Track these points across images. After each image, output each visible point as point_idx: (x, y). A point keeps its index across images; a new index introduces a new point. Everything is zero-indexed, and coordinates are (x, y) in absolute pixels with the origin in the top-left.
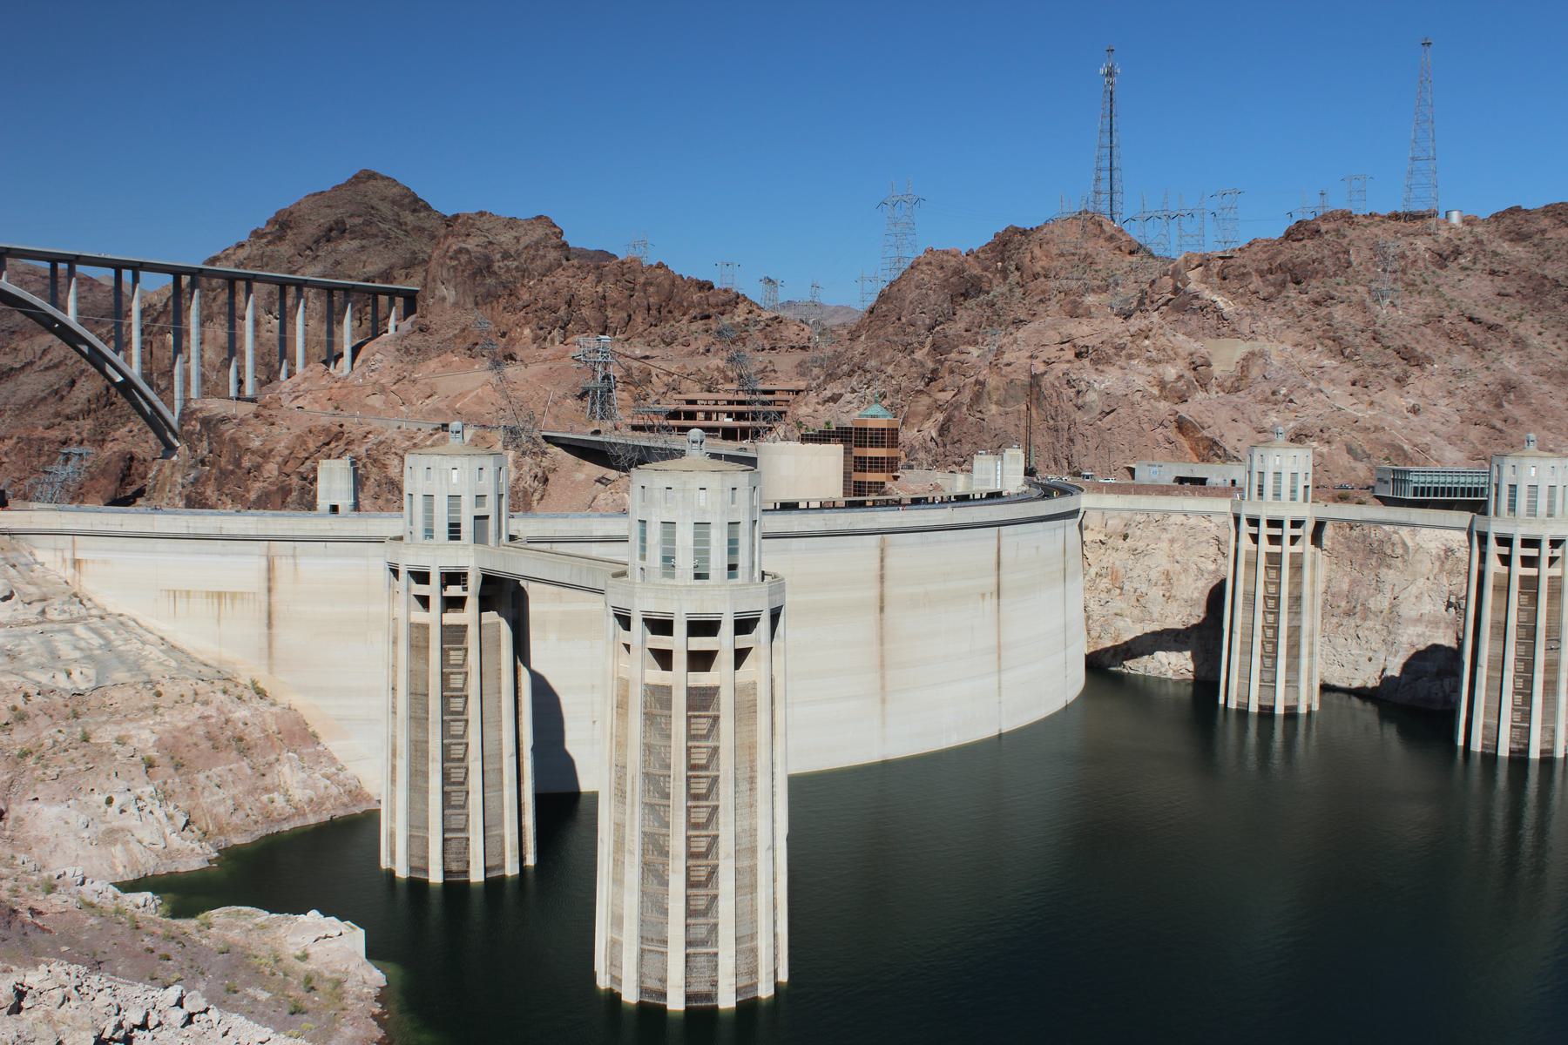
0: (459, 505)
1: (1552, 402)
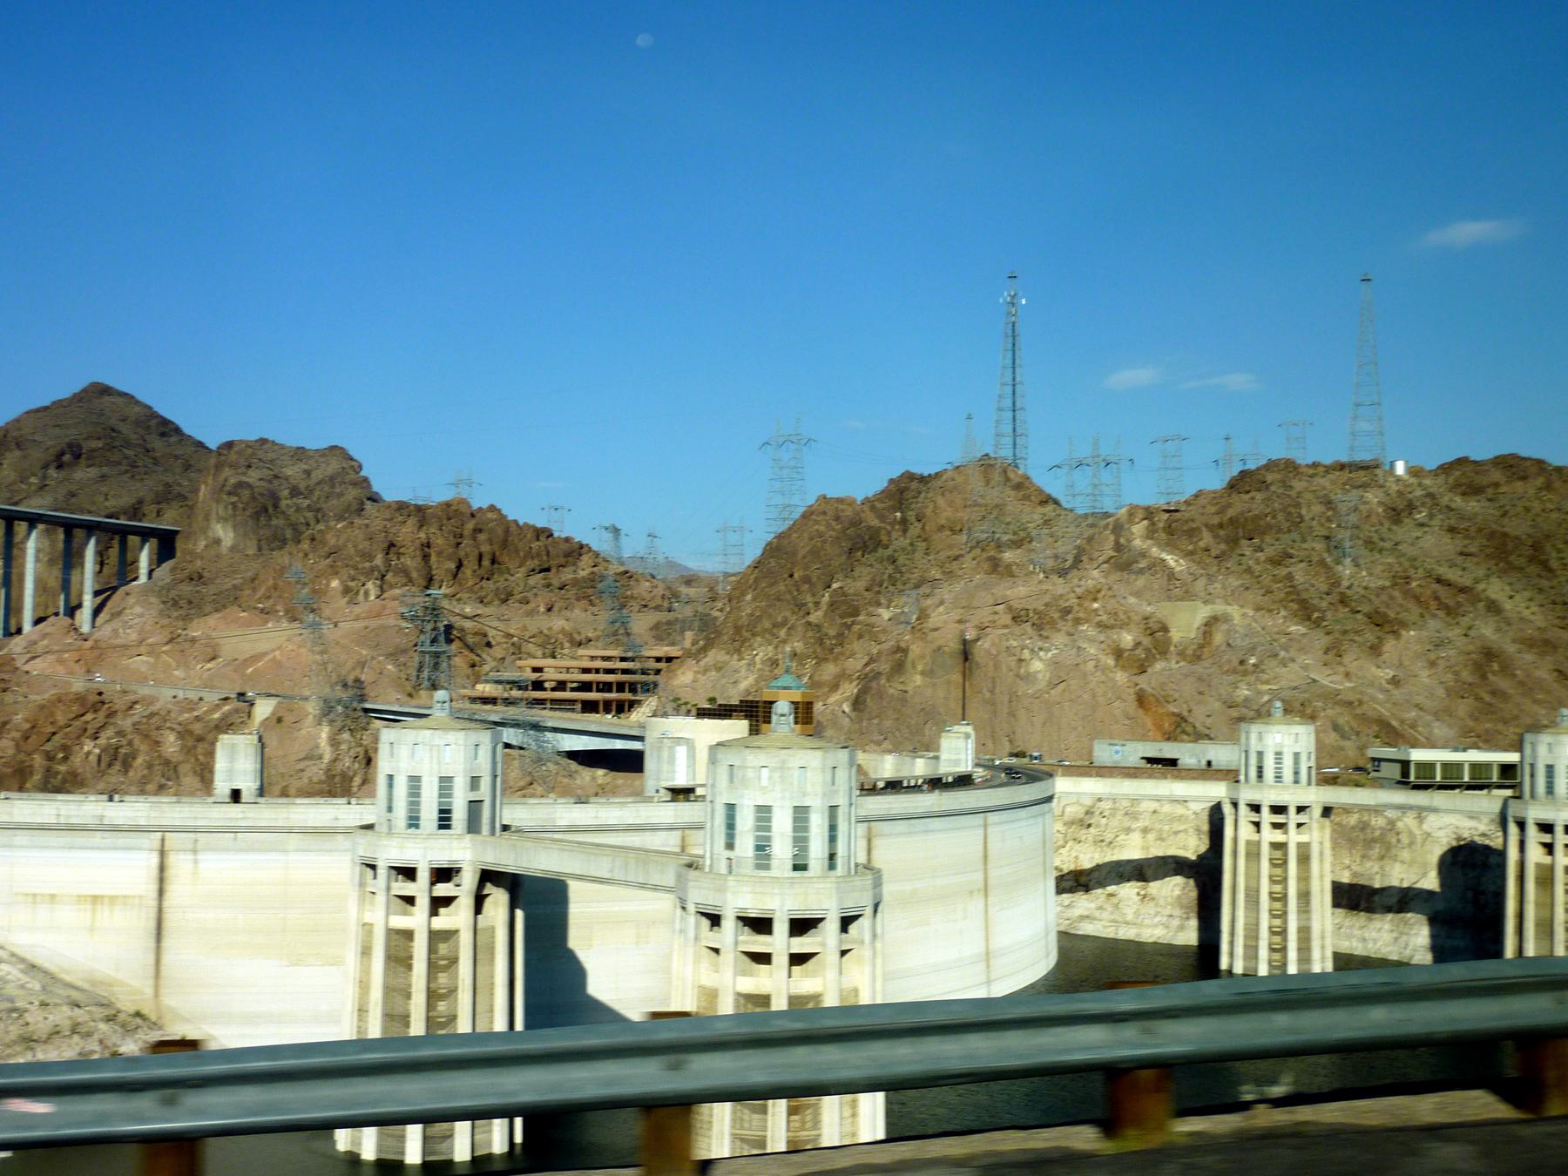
0: (451, 788)
1: (1538, 673)
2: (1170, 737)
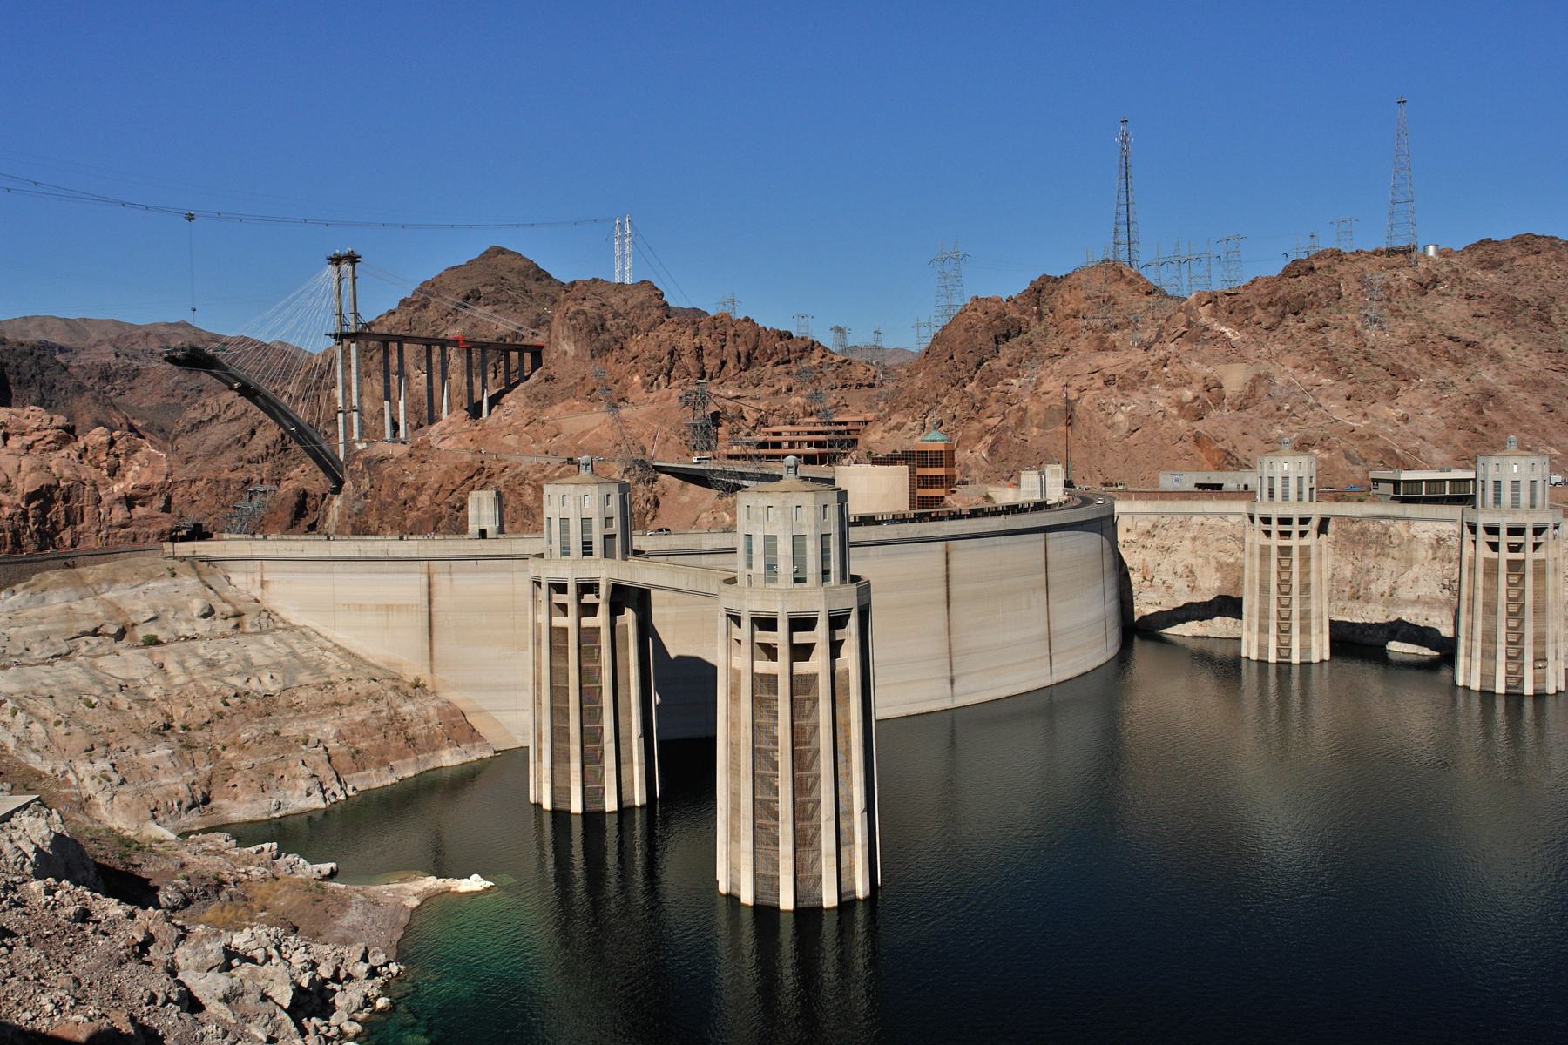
2: (1220, 468)
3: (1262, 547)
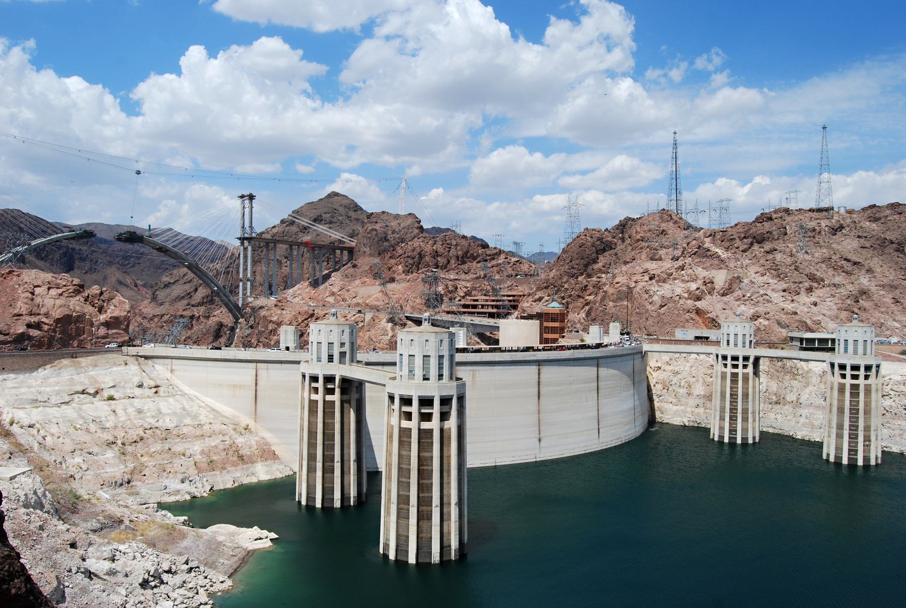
3: (722, 373)
